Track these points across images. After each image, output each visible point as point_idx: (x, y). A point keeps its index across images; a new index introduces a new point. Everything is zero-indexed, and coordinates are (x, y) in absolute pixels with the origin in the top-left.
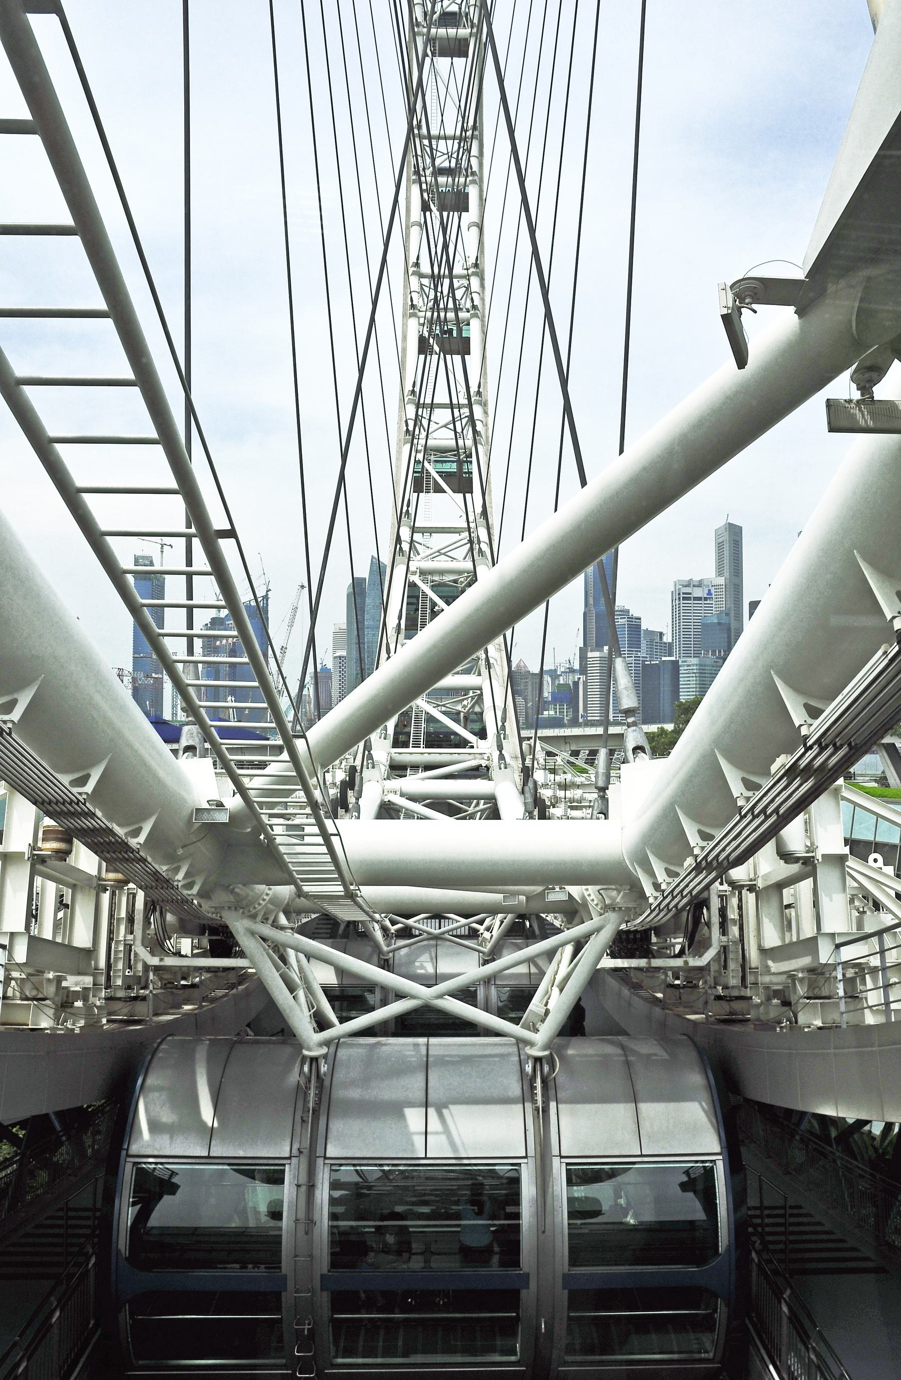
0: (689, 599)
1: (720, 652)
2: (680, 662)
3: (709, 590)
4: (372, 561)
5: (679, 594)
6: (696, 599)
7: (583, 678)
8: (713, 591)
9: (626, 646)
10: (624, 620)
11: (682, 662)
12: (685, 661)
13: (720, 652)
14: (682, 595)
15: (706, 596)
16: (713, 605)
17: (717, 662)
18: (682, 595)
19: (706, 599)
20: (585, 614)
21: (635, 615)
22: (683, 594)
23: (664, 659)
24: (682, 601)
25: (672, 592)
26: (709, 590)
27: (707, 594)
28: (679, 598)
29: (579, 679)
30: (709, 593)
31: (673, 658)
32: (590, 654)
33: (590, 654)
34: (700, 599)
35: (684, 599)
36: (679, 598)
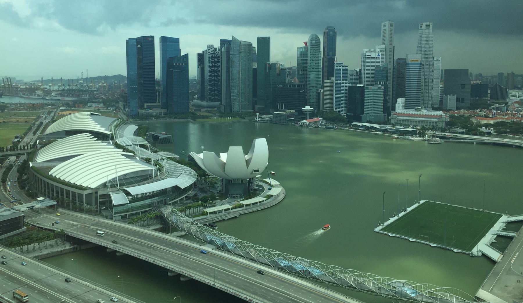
0: (369, 58)
1: (383, 83)
3: (379, 54)
5: (365, 56)
6: (372, 58)
7: (322, 90)
8: (380, 54)
10: (341, 67)
13: (383, 83)
14: (366, 56)
15: (377, 56)
16: (380, 61)
18: (366, 56)
19: (377, 58)
22: (367, 55)
23: (358, 85)
24: (366, 59)
25: (362, 54)
26: (379, 54)
27: (378, 56)
30: (379, 55)
31: (362, 85)
32: (325, 81)
33: (325, 81)
34: (374, 58)
35: (367, 58)
36: (365, 57)
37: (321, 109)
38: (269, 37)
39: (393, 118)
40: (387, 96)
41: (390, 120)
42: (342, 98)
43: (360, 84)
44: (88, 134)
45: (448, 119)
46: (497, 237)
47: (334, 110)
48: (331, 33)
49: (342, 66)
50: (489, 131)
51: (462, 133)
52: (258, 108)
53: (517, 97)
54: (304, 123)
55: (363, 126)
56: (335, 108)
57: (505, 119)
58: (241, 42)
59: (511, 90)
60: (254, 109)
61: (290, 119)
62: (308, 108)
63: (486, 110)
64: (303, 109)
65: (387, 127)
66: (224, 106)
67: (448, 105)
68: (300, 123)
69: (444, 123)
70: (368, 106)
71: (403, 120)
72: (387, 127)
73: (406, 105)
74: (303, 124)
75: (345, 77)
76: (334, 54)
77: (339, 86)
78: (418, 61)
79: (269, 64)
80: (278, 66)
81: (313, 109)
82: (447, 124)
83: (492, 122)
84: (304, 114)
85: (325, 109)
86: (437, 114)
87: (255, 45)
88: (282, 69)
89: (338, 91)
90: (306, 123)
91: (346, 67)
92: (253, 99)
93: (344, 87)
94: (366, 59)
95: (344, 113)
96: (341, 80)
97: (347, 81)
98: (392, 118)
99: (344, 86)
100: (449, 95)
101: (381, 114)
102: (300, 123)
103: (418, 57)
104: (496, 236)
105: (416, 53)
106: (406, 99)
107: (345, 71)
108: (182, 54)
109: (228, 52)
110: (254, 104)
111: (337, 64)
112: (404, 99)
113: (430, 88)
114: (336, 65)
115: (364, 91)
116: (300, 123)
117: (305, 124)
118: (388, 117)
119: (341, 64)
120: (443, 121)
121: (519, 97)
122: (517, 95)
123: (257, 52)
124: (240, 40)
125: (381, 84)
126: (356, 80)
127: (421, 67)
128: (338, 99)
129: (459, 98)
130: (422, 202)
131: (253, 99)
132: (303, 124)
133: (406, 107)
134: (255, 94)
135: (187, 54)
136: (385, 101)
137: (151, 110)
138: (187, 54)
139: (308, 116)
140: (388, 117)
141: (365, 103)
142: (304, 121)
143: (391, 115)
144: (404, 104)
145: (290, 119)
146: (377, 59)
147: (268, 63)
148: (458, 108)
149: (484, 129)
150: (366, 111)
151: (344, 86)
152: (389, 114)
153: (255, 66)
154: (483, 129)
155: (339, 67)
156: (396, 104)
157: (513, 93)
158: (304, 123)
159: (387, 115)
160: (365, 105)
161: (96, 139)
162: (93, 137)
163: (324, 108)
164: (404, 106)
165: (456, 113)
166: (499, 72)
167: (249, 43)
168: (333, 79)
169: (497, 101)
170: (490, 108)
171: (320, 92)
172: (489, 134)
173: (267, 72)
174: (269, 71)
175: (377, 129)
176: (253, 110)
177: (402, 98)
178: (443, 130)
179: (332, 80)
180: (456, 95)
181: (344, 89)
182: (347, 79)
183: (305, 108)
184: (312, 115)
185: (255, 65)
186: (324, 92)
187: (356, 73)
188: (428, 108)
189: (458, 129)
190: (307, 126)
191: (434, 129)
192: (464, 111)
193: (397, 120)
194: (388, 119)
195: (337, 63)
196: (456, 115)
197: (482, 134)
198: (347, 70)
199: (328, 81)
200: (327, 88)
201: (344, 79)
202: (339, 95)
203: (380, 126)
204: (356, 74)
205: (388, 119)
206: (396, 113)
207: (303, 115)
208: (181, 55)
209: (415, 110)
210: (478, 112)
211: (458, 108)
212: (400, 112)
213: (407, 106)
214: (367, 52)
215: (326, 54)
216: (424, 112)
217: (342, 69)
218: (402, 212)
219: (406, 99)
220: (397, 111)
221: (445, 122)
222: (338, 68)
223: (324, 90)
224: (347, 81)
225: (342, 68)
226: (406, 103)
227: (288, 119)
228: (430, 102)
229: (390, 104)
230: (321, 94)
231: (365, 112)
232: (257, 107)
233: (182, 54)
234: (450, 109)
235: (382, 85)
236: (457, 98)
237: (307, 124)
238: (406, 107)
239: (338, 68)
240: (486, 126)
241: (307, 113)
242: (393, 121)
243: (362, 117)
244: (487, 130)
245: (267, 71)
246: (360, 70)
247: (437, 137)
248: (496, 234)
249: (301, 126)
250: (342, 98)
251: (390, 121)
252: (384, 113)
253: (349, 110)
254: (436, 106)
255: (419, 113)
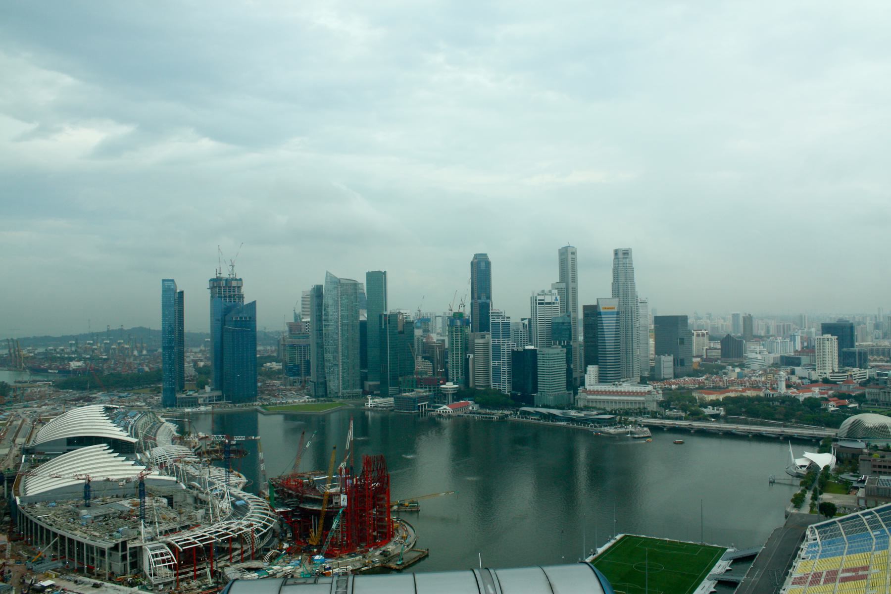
0: (542, 304)
1: (564, 343)
2: (538, 352)
3: (556, 298)
4: (327, 275)
7: (472, 356)
9: (501, 328)
11: (539, 351)
12: (541, 351)
13: (564, 343)
14: (538, 302)
17: (561, 351)
19: (554, 303)
20: (472, 304)
21: (507, 316)
22: (539, 300)
23: (527, 347)
24: (538, 306)
25: (531, 297)
26: (556, 298)
27: (555, 300)
28: (536, 303)
29: (469, 356)
30: (556, 299)
31: (532, 347)
33: (476, 341)
34: (550, 303)
35: (539, 304)
36: (536, 303)
37: (471, 385)
38: (385, 272)
39: (582, 397)
40: (572, 363)
41: (577, 401)
42: (503, 367)
43: (530, 342)
44: (104, 446)
45: (660, 398)
46: (718, 583)
47: (492, 388)
48: (483, 265)
49: (501, 317)
50: (718, 412)
51: (679, 418)
52: (370, 385)
53: (758, 353)
54: (444, 411)
55: (537, 413)
56: (493, 384)
57: (740, 391)
58: (341, 280)
59: (749, 341)
60: (362, 387)
61: (421, 404)
62: (449, 385)
63: (715, 376)
64: (441, 388)
65: (573, 413)
66: (315, 385)
67: (662, 370)
68: (439, 411)
69: (655, 403)
70: (544, 381)
71: (596, 401)
72: (573, 413)
73: (600, 376)
74: (443, 412)
75: (507, 335)
76: (489, 297)
77: (497, 348)
78: (614, 308)
79: (386, 315)
80: (400, 318)
81: (457, 386)
82: (660, 404)
83: (721, 397)
84: (445, 395)
85: (478, 386)
86: (645, 389)
87: (362, 280)
88: (407, 322)
89: (497, 357)
90: (447, 411)
91: (508, 319)
92: (362, 370)
93: (506, 351)
94: (538, 306)
95: (508, 392)
96: (501, 339)
97: (510, 340)
98: (580, 398)
99: (506, 348)
100: (662, 356)
101: (564, 392)
102: (439, 411)
103: (615, 303)
104: (716, 582)
105: (611, 297)
106: (600, 366)
107: (507, 325)
108: (247, 301)
109: (320, 296)
110: (364, 378)
111: (493, 314)
112: (597, 366)
113: (635, 345)
114: (492, 316)
115: (537, 357)
116: (437, 411)
117: (446, 412)
118: (574, 397)
119: (499, 315)
120: (653, 401)
121: (760, 353)
122: (758, 350)
123: (365, 292)
124: (339, 277)
125: (562, 344)
126: (524, 335)
127: (619, 317)
128: (497, 371)
129: (677, 361)
130: (619, 537)
131: (362, 370)
132: (443, 412)
133: (600, 379)
134: (364, 363)
135: (254, 304)
136: (569, 372)
137: (196, 394)
138: (253, 305)
139: (450, 398)
140: (574, 397)
141: (539, 375)
142: (445, 407)
143: (579, 394)
144: (597, 375)
145: (421, 404)
146: (554, 305)
147: (385, 313)
148: (676, 376)
149: (711, 409)
150: (540, 387)
151: (506, 348)
152: (576, 393)
153: (363, 315)
154: (709, 411)
155: (497, 318)
156: (586, 375)
157: (753, 347)
158: (444, 411)
159: (572, 392)
160: (539, 375)
161: (117, 454)
162: (108, 447)
163: (477, 384)
164: (597, 378)
165: (674, 383)
166: (733, 313)
167: (353, 282)
168: (489, 337)
169: (730, 360)
170: (720, 373)
171: (468, 359)
172: (716, 417)
173: (383, 327)
174: (386, 327)
175: (558, 418)
176: (361, 390)
177: (594, 366)
178: (654, 415)
179: (486, 339)
180: (672, 355)
181: (506, 353)
182: (510, 338)
183: (445, 384)
184: (458, 395)
185: (363, 316)
186: (474, 358)
187: (523, 327)
188: (633, 377)
189: (674, 413)
190: (449, 415)
191: (642, 412)
192: (684, 380)
193: (588, 401)
194: (574, 399)
195: (494, 313)
196: (673, 387)
197: (705, 418)
198: (509, 323)
199: (481, 341)
200: (480, 353)
201: (505, 338)
202: (495, 365)
203: (561, 411)
204: (524, 328)
205: (574, 399)
206: (585, 391)
207: (440, 397)
208: (245, 303)
209: (614, 385)
210: (704, 380)
211: (676, 376)
212: (592, 388)
213: (602, 378)
214: (538, 295)
215: (476, 296)
216: (626, 387)
217: (501, 321)
218: (590, 555)
219: (600, 366)
220: (587, 387)
221: (657, 401)
222: (494, 320)
223: (474, 356)
224: (510, 340)
225: (502, 320)
226: (600, 373)
227: (419, 404)
228: (636, 367)
229: (575, 375)
230: (470, 362)
231: (539, 390)
232: (369, 383)
233: (247, 301)
234: (666, 377)
235: (563, 347)
236: (674, 359)
237: (449, 412)
238: (600, 379)
239: (494, 320)
240: (714, 404)
241: (448, 394)
242: (581, 404)
243: (535, 397)
244: (715, 412)
245: (383, 325)
246: (530, 320)
247: (645, 426)
248: (716, 580)
249: (440, 416)
250: (503, 367)
251: (577, 405)
252: (568, 389)
253: (514, 387)
254: (646, 374)
255: (619, 389)
